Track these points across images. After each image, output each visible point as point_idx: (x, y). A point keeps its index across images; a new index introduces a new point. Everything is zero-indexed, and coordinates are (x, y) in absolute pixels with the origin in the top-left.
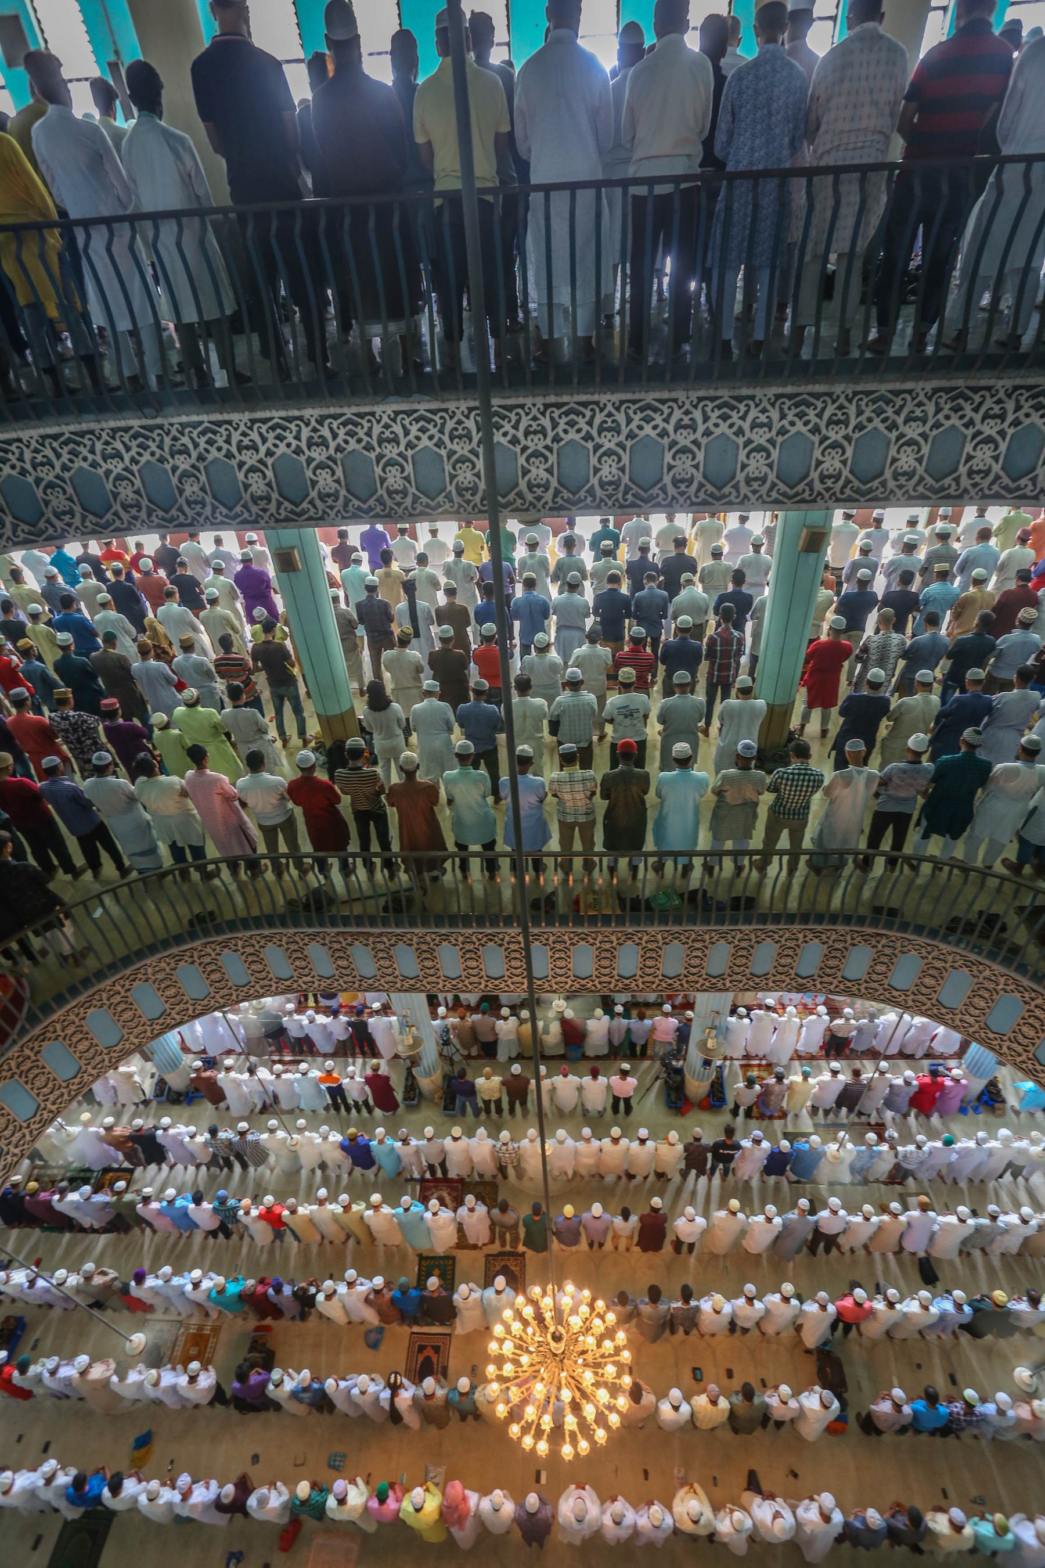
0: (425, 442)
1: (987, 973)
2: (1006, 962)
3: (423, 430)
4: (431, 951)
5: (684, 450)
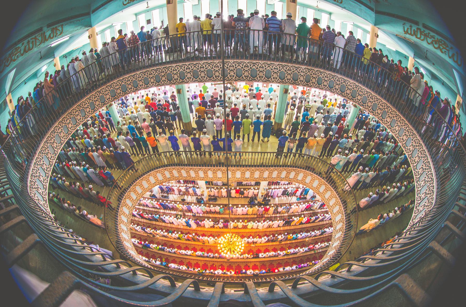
5: (261, 71)
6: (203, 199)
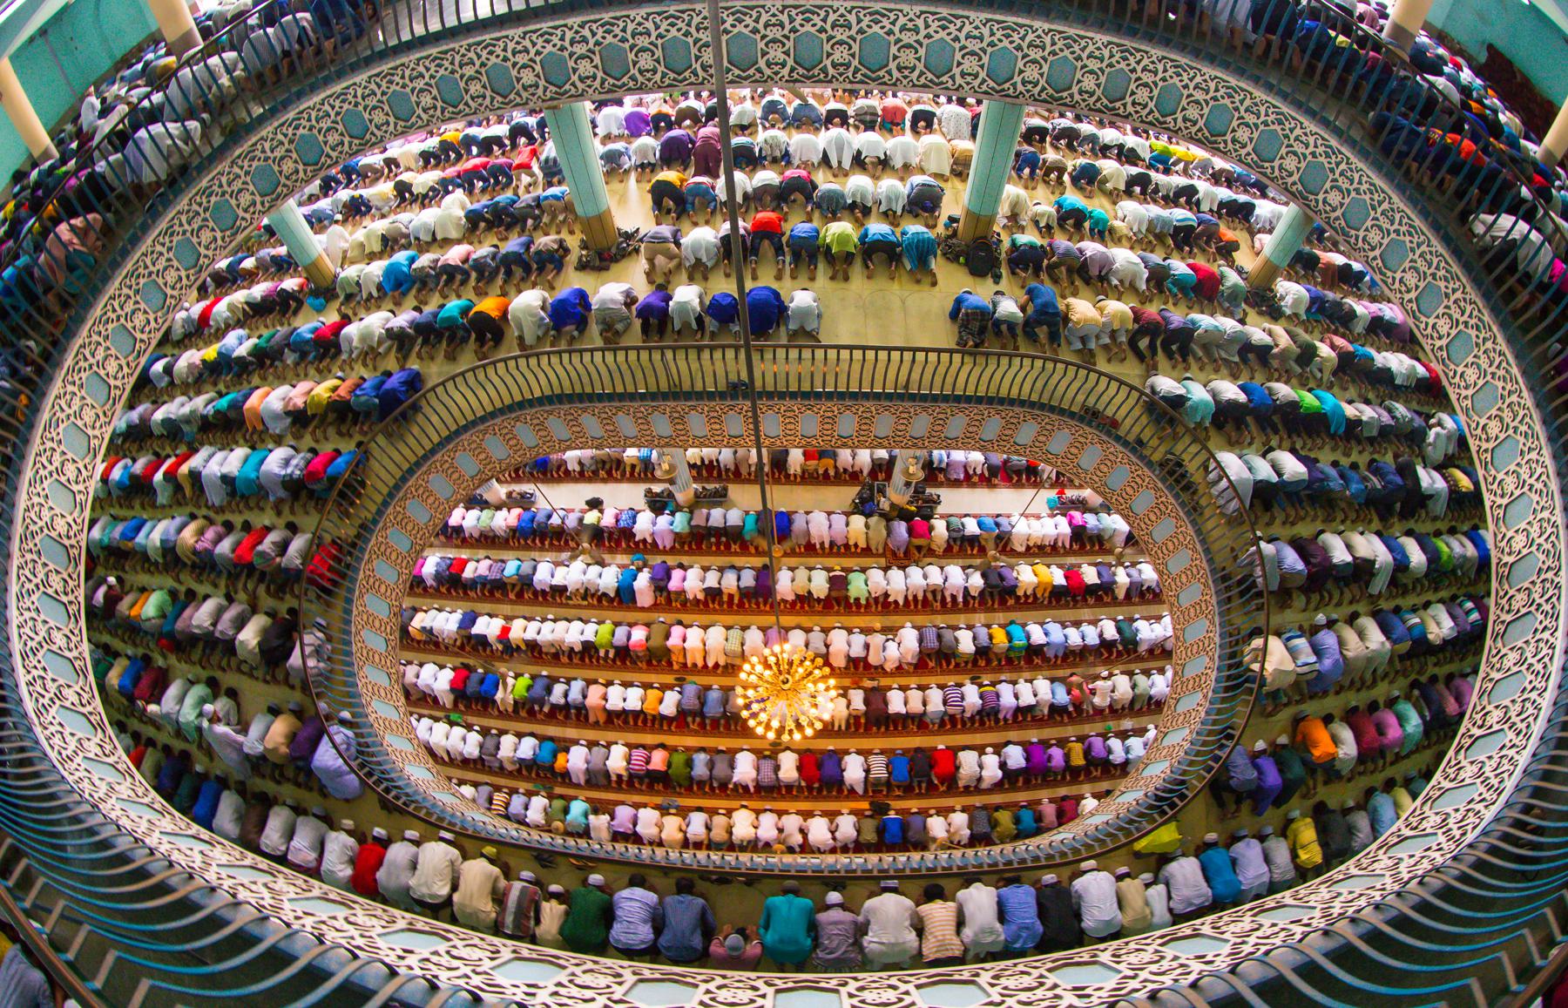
0: (674, 31)
3: (672, 25)
6: (671, 495)
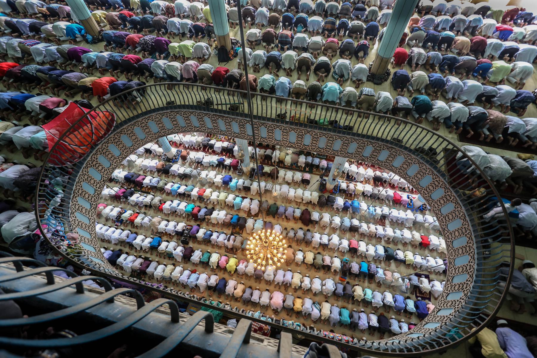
1: (424, 167)
2: (431, 164)
4: (243, 125)
